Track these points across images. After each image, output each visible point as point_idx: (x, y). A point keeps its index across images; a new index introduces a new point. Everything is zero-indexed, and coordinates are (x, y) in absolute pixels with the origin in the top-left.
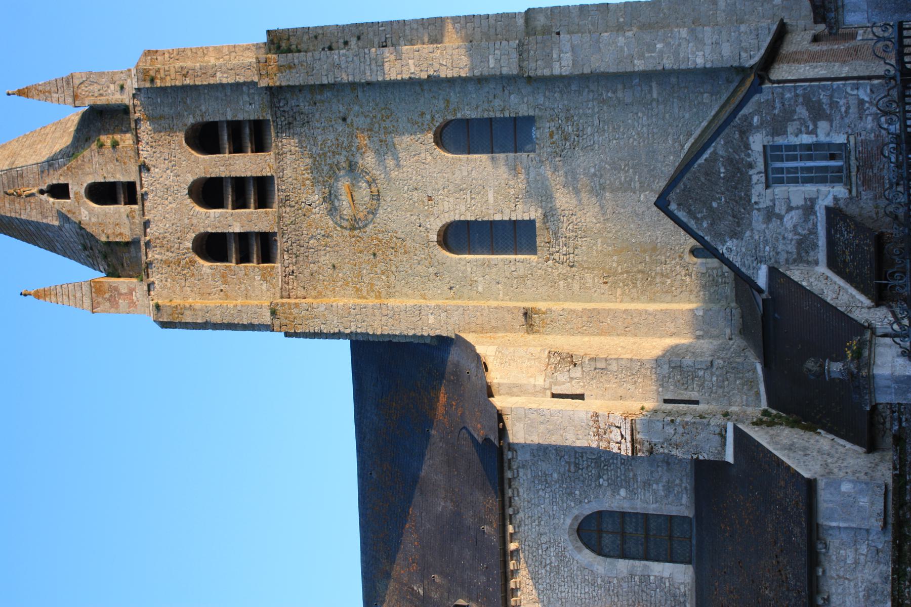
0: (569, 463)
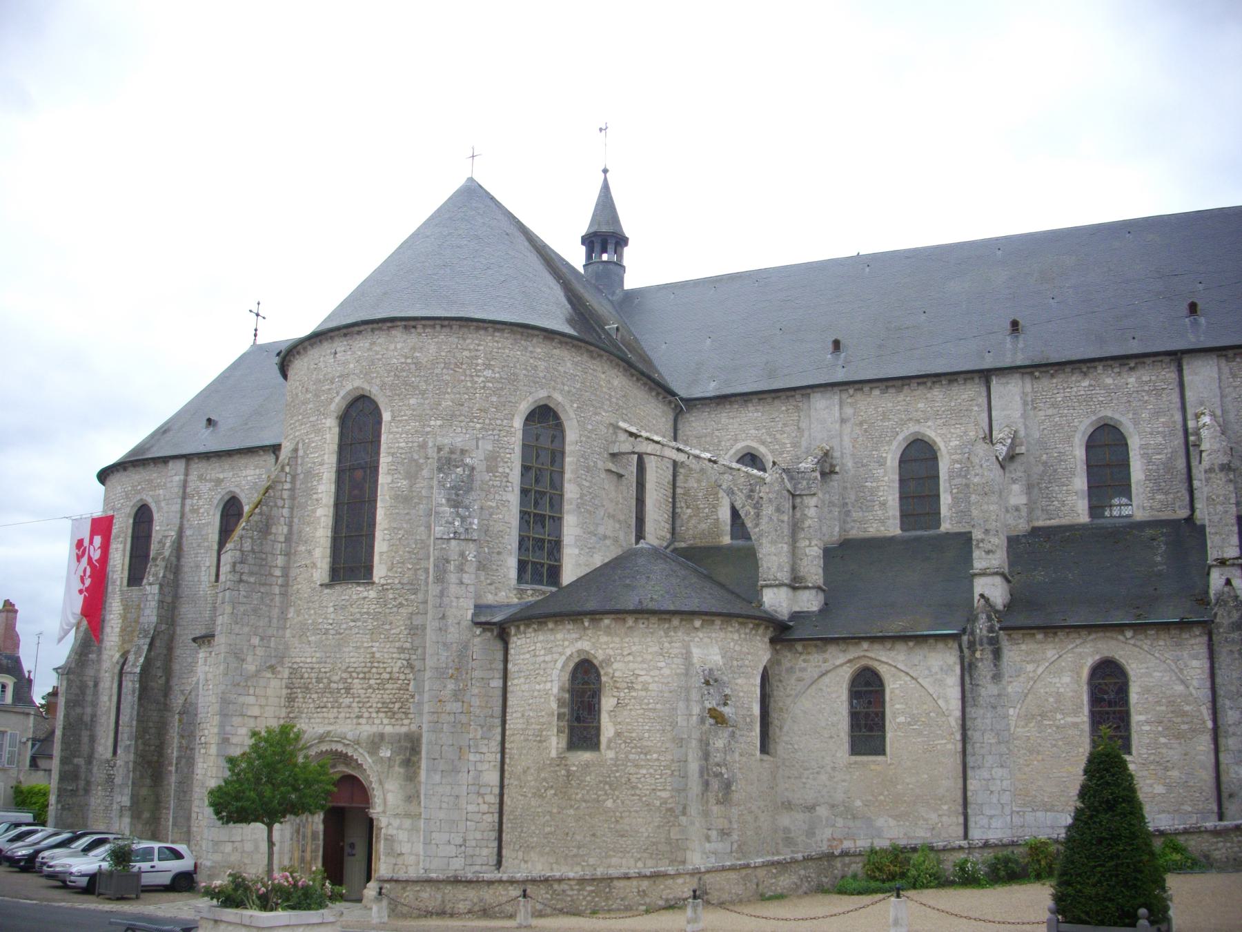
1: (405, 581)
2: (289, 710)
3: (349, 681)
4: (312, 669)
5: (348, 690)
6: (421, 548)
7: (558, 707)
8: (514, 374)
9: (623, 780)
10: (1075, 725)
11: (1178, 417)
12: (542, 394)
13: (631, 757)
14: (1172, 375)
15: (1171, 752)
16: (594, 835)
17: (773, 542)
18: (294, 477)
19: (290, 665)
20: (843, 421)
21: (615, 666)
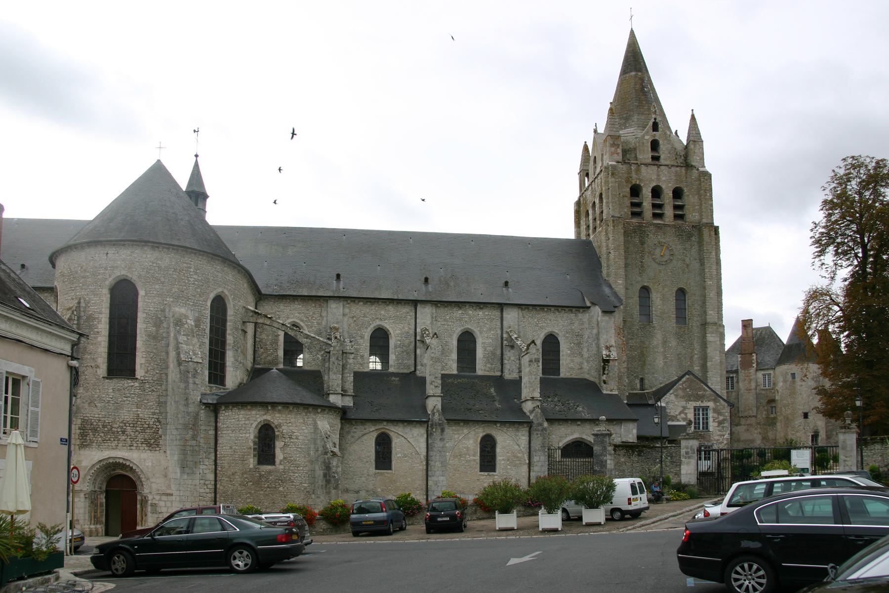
0: (579, 332)
1: (155, 379)
2: (83, 440)
3: (124, 427)
4: (99, 420)
5: (124, 432)
6: (164, 363)
7: (254, 445)
8: (208, 279)
9: (288, 479)
10: (474, 460)
11: (499, 332)
12: (220, 290)
13: (291, 468)
14: (498, 313)
15: (512, 472)
16: (274, 503)
17: (334, 373)
18: (79, 318)
19: (82, 417)
20: (344, 315)
21: (283, 427)
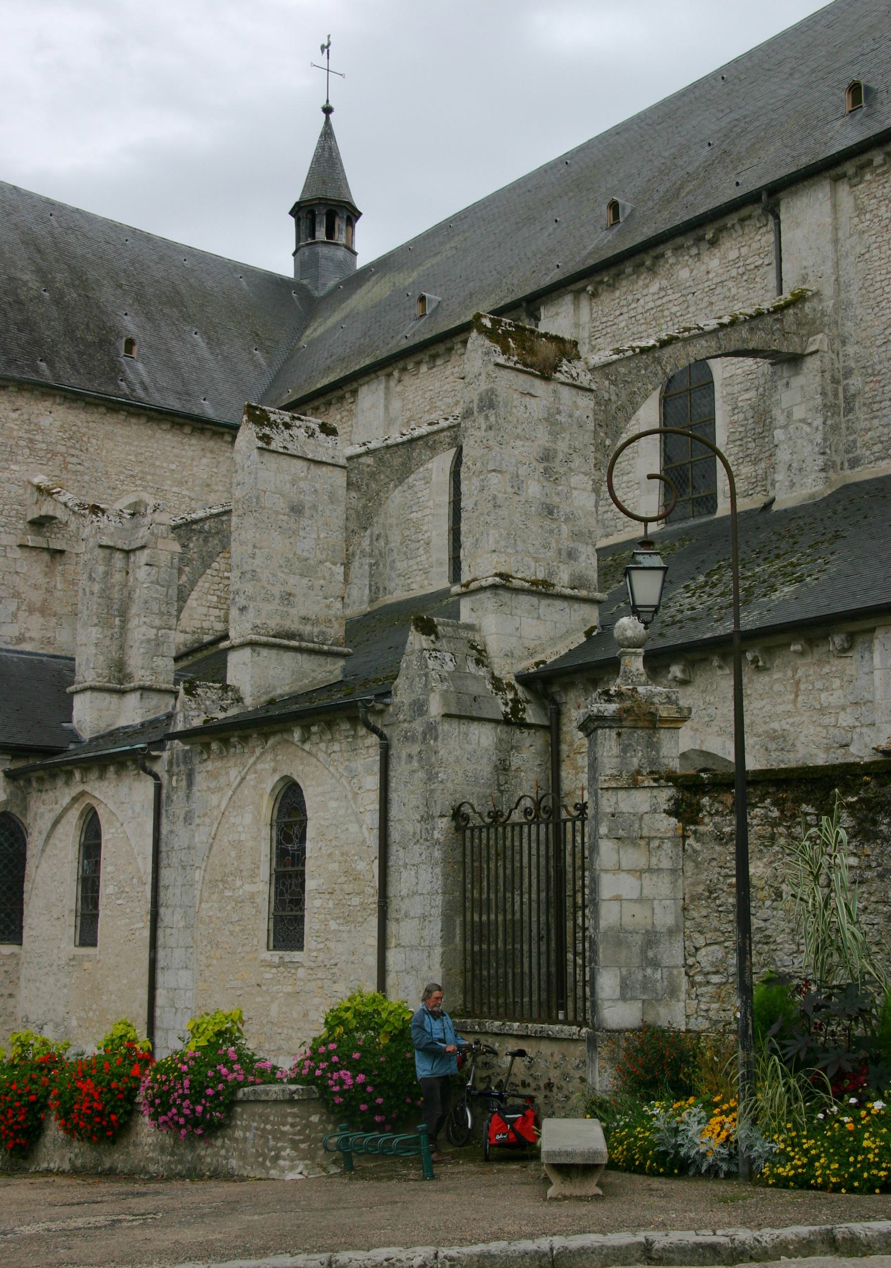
10: (252, 897)
